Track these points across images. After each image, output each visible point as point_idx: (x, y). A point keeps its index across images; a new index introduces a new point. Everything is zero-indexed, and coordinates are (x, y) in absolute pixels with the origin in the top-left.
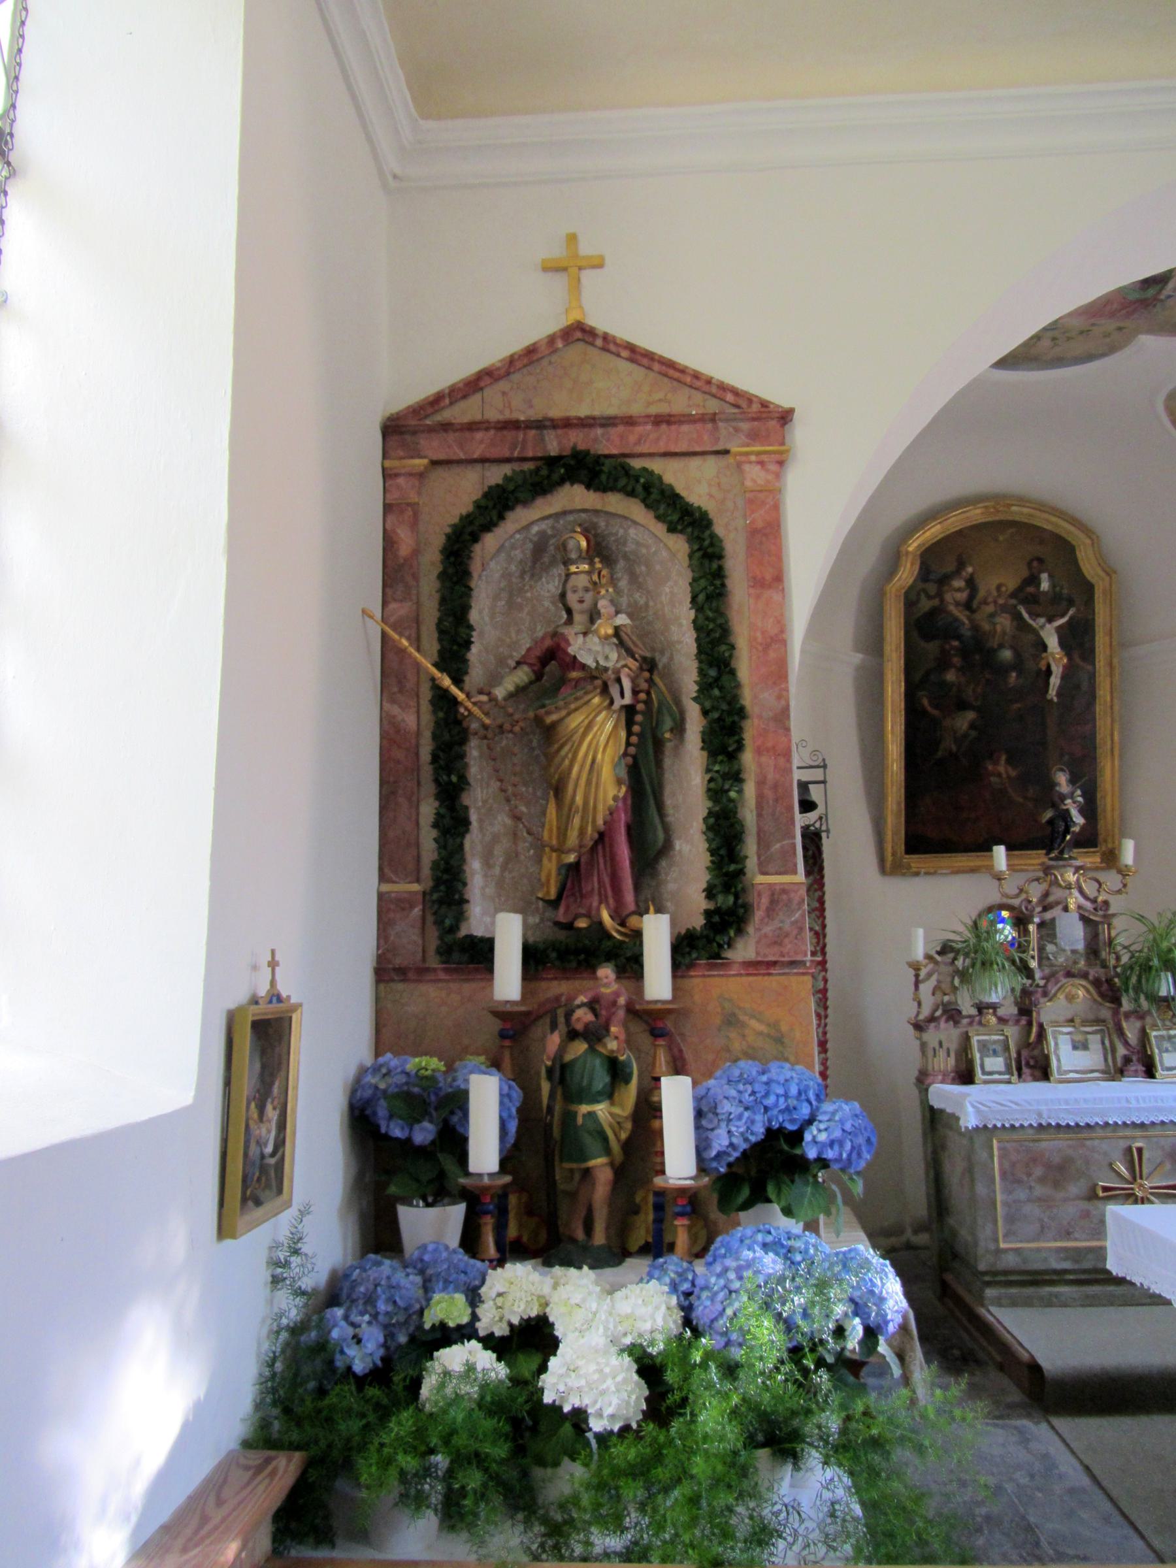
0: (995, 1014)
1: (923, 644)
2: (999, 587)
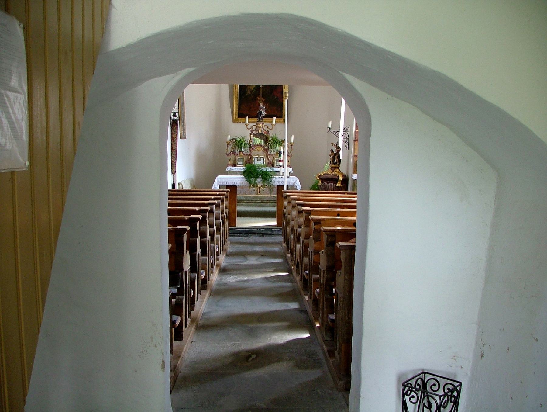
0: (242, 153)
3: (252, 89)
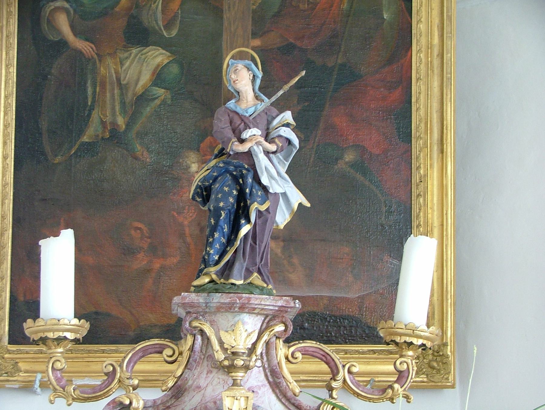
3: (139, 89)
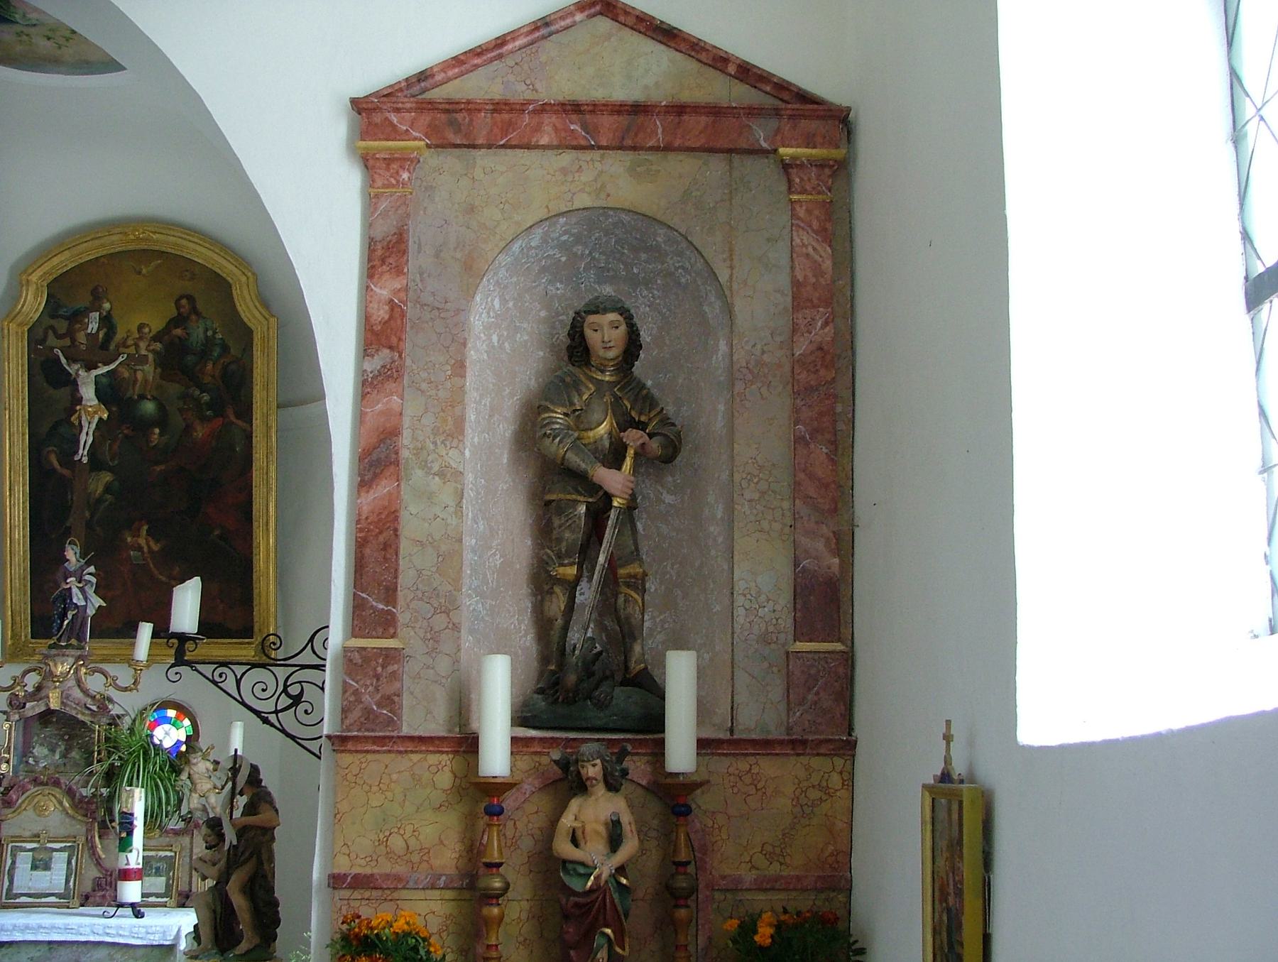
1: (51, 391)
2: (141, 327)
